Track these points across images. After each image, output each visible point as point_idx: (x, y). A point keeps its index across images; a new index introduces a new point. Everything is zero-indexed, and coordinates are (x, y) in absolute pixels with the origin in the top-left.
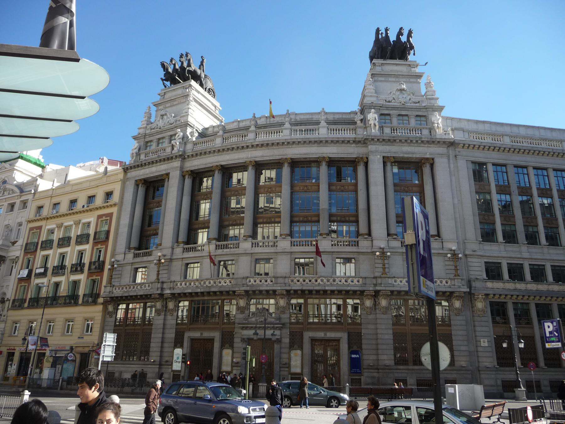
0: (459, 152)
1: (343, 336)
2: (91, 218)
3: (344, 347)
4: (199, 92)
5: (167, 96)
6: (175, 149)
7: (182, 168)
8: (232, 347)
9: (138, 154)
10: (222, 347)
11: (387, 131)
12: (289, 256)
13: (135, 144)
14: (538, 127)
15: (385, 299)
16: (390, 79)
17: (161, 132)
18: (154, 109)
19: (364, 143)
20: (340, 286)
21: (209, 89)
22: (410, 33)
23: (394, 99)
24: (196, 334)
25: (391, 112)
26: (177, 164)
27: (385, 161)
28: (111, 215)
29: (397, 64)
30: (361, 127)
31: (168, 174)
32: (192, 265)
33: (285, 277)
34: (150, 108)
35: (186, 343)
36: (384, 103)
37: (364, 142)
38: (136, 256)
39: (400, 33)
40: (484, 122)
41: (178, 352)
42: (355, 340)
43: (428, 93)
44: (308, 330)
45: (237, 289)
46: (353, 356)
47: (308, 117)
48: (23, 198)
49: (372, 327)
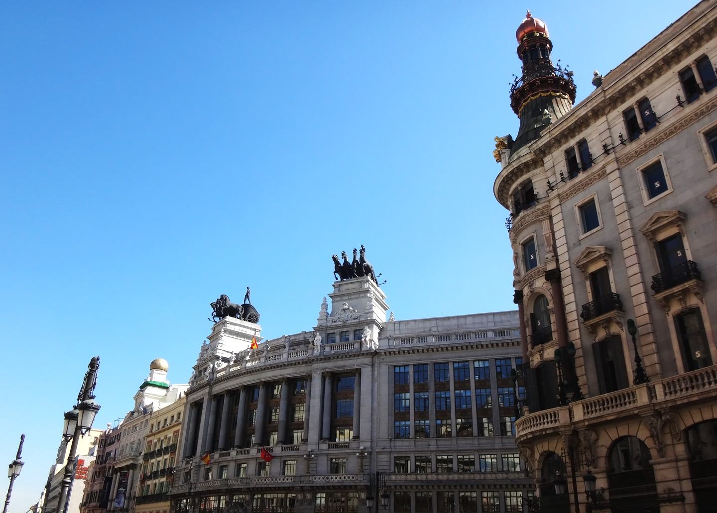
0: (383, 359)
2: (170, 434)
4: (235, 324)
5: (216, 329)
7: (210, 393)
9: (193, 382)
11: (327, 349)
12: (255, 461)
13: (190, 373)
14: (486, 314)
20: (279, 483)
23: (339, 318)
26: (207, 390)
28: (177, 431)
29: (351, 283)
31: (203, 398)
33: (247, 478)
34: (205, 341)
37: (309, 362)
38: (187, 463)
40: (430, 320)
45: (222, 488)
48: (146, 418)
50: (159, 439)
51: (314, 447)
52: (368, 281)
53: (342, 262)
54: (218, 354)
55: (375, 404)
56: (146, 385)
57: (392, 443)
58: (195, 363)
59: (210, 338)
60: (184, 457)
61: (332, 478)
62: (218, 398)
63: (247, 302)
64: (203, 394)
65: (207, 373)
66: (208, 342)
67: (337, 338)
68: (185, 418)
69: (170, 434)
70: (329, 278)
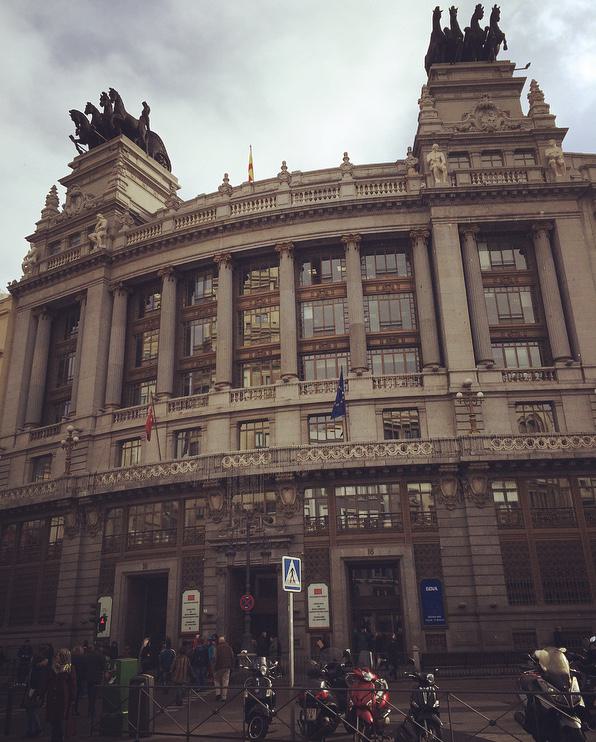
1: (403, 551)
3: (409, 575)
4: (137, 157)
6: (95, 247)
8: (200, 586)
10: (184, 587)
15: (479, 479)
16: (464, 95)
17: (74, 225)
18: (62, 191)
19: (422, 205)
21: (158, 154)
22: (496, 13)
23: (473, 124)
24: (138, 567)
27: (463, 231)
30: (415, 178)
32: (129, 444)
34: (54, 188)
35: (120, 584)
36: (456, 132)
37: (424, 202)
38: (34, 436)
39: (479, 13)
41: (106, 603)
42: (429, 558)
43: (535, 111)
44: (339, 543)
46: (428, 589)
58: (32, 230)
60: (23, 424)
61: (541, 443)
62: (139, 290)
65: (98, 234)
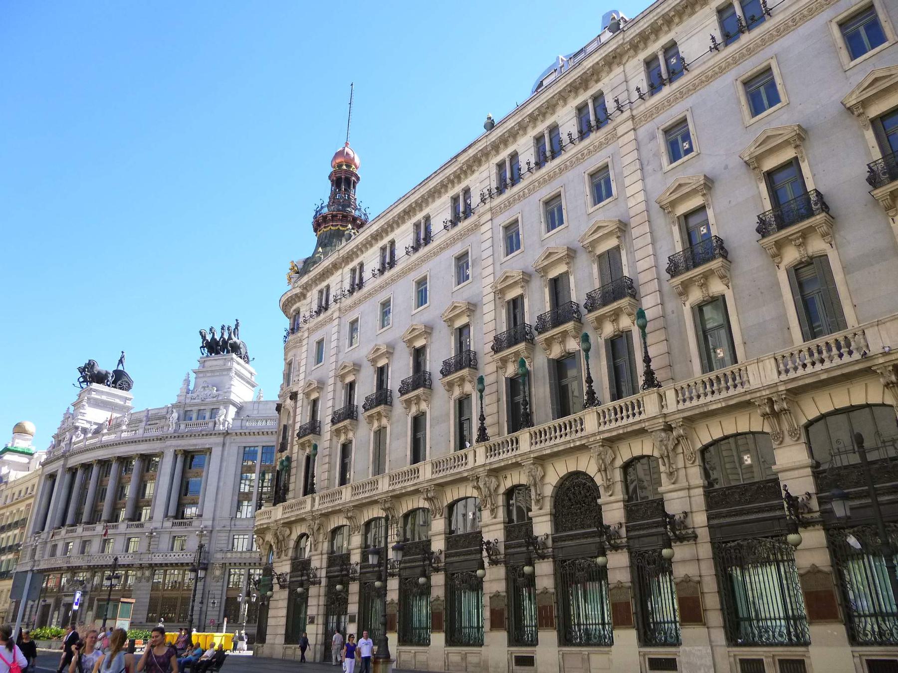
2: (22, 507)
4: (102, 393)
7: (64, 465)
25: (193, 408)
26: (61, 462)
28: (29, 505)
47: (156, 411)
49: (138, 592)
50: (11, 513)
51: (159, 525)
52: (232, 359)
53: (209, 337)
54: (77, 424)
55: (221, 484)
56: (6, 450)
57: (233, 522)
59: (74, 405)
62: (73, 471)
63: (120, 368)
64: (57, 466)
66: (72, 408)
67: (194, 416)
68: (38, 491)
69: (22, 507)
70: (193, 353)
